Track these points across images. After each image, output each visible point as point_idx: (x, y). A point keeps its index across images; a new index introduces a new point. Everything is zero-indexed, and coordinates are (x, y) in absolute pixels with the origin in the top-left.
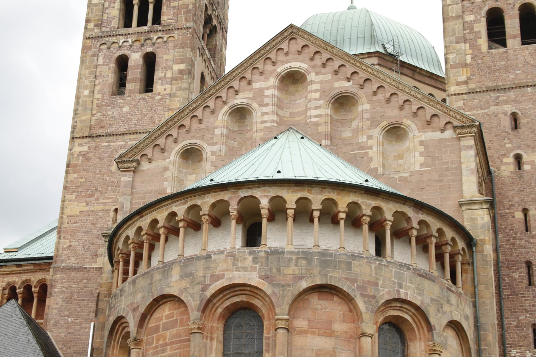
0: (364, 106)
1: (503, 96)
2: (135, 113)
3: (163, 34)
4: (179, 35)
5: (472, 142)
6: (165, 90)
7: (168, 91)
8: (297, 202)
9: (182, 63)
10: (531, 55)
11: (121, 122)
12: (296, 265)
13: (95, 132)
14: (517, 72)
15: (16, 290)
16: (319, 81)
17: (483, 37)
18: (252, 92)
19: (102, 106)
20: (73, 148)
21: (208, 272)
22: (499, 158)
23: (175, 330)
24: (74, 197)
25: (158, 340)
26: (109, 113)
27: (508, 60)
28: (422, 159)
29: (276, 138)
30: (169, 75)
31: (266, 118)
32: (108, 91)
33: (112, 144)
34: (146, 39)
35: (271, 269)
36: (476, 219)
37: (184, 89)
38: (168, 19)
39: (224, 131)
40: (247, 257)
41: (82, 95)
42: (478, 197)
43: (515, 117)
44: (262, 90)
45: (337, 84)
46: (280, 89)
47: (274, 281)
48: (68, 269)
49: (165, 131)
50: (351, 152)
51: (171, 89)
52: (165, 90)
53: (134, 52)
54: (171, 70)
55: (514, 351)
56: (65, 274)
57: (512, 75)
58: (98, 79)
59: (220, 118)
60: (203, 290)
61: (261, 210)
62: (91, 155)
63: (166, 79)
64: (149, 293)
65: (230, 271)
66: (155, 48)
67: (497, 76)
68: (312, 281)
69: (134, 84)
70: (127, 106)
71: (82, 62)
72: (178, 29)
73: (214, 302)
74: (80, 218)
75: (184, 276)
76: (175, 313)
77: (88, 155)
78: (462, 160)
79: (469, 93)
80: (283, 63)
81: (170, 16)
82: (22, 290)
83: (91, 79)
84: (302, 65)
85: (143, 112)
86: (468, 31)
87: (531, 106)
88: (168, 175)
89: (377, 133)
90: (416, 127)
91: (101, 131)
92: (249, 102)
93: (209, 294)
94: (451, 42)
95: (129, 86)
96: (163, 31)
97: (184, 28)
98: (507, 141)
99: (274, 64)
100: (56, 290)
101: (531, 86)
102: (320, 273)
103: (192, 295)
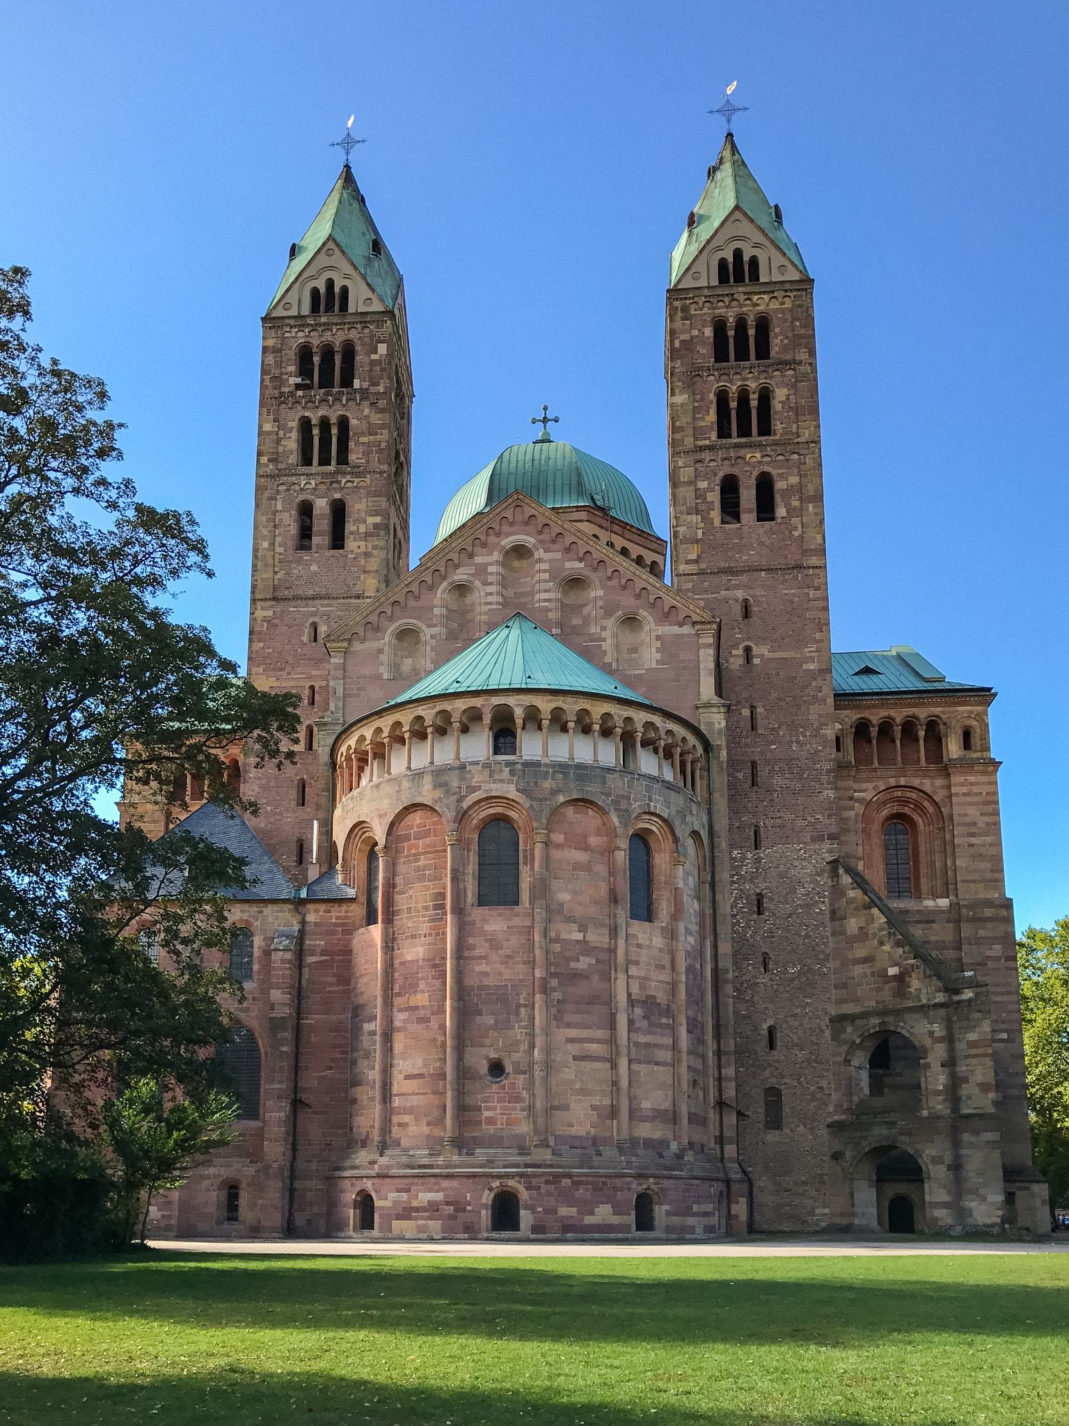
0: (596, 593)
4: (371, 479)
5: (711, 640)
6: (359, 547)
13: (279, 594)
23: (428, 840)
24: (261, 670)
25: (409, 850)
28: (658, 656)
30: (362, 529)
31: (490, 599)
32: (290, 543)
34: (333, 482)
39: (444, 611)
42: (716, 700)
44: (486, 565)
45: (568, 565)
46: (503, 565)
49: (377, 607)
52: (359, 547)
59: (439, 595)
60: (459, 801)
71: (257, 506)
75: (435, 787)
80: (508, 535)
84: (529, 541)
88: (383, 658)
89: (610, 623)
92: (471, 578)
93: (465, 805)
94: (682, 513)
99: (498, 535)
103: (447, 806)
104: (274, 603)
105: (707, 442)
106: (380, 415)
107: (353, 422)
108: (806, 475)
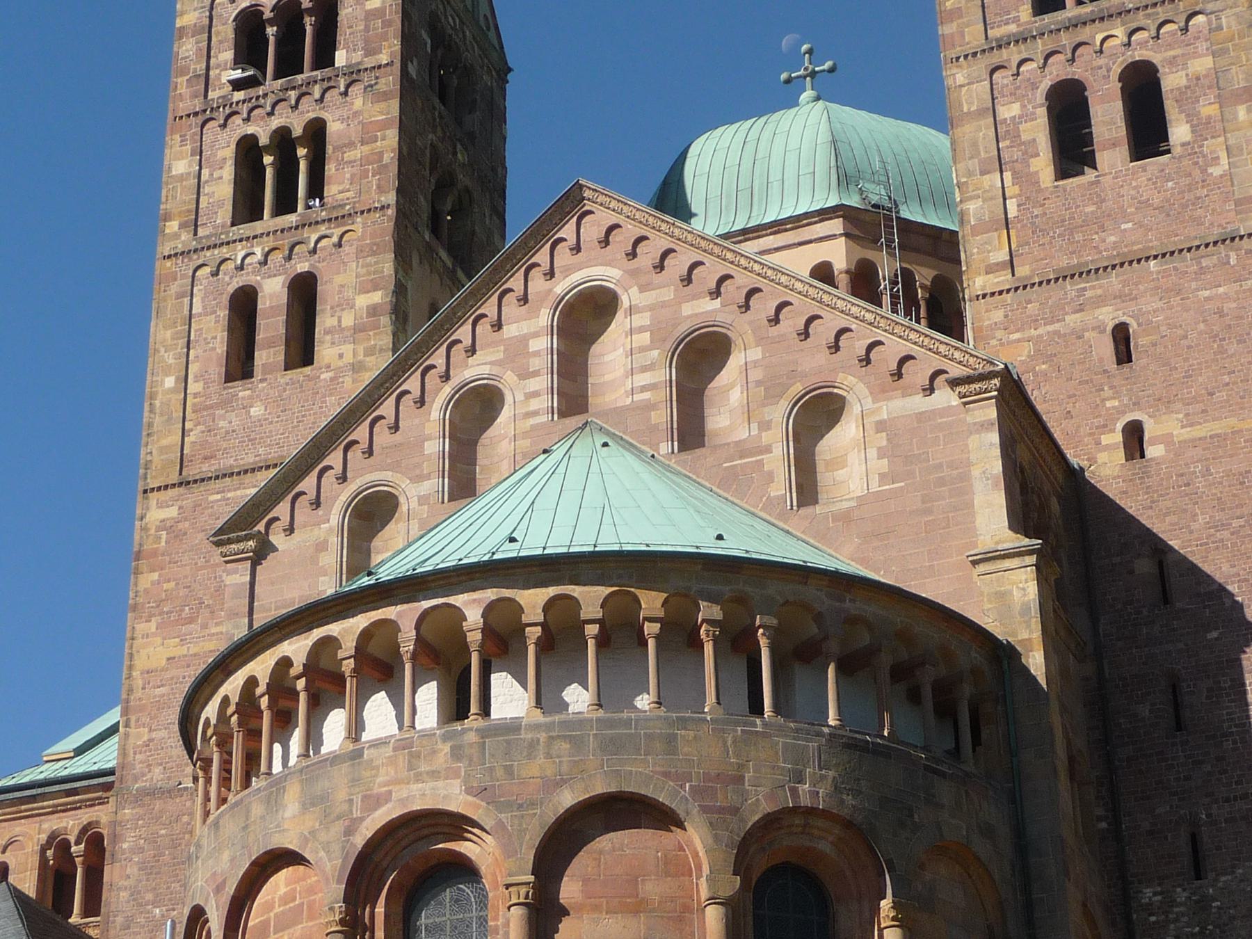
1: (1093, 288)
3: (330, 228)
4: (365, 225)
6: (341, 356)
7: (349, 358)
8: (549, 606)
10: (1155, 183)
11: (249, 440)
12: (548, 755)
13: (191, 472)
14: (1123, 227)
15: (70, 847)
16: (648, 306)
17: (1041, 154)
18: (502, 348)
19: (207, 408)
20: (145, 514)
21: (357, 790)
22: (1091, 434)
24: (153, 626)
26: (222, 424)
27: (1103, 201)
29: (545, 451)
30: (348, 320)
31: (535, 404)
33: (229, 495)
35: (491, 769)
36: (1011, 592)
37: (381, 350)
40: (440, 746)
41: (160, 390)
43: (1121, 335)
44: (524, 340)
45: (687, 309)
47: (500, 797)
48: (148, 794)
50: (725, 465)
52: (341, 356)
53: (269, 277)
54: (351, 308)
55: (1148, 892)
56: (142, 806)
57: (1112, 235)
60: (349, 832)
61: (468, 634)
62: (187, 524)
63: (343, 329)
64: (243, 847)
65: (403, 783)
66: (316, 262)
67: (1078, 242)
68: (586, 789)
69: (272, 350)
70: (259, 403)
72: (362, 212)
73: (376, 858)
74: (168, 675)
75: (308, 803)
76: (298, 889)
77: (180, 526)
78: (973, 457)
79: (1017, 289)
80: (568, 271)
81: (344, 182)
82: (82, 846)
83: (179, 350)
85: (294, 413)
86: (1008, 143)
87: (1160, 304)
89: (779, 413)
90: (867, 391)
91: (207, 468)
92: (496, 370)
93: (359, 841)
94: (970, 174)
95: (262, 357)
96: (330, 220)
97: (376, 208)
98: (1107, 392)
99: (551, 274)
100: (125, 846)
101: (1156, 257)
102: (603, 768)
103: (326, 847)
104: (182, 490)
105: (1013, 28)
106: (383, 105)
107: (334, 128)
108: (1225, 51)
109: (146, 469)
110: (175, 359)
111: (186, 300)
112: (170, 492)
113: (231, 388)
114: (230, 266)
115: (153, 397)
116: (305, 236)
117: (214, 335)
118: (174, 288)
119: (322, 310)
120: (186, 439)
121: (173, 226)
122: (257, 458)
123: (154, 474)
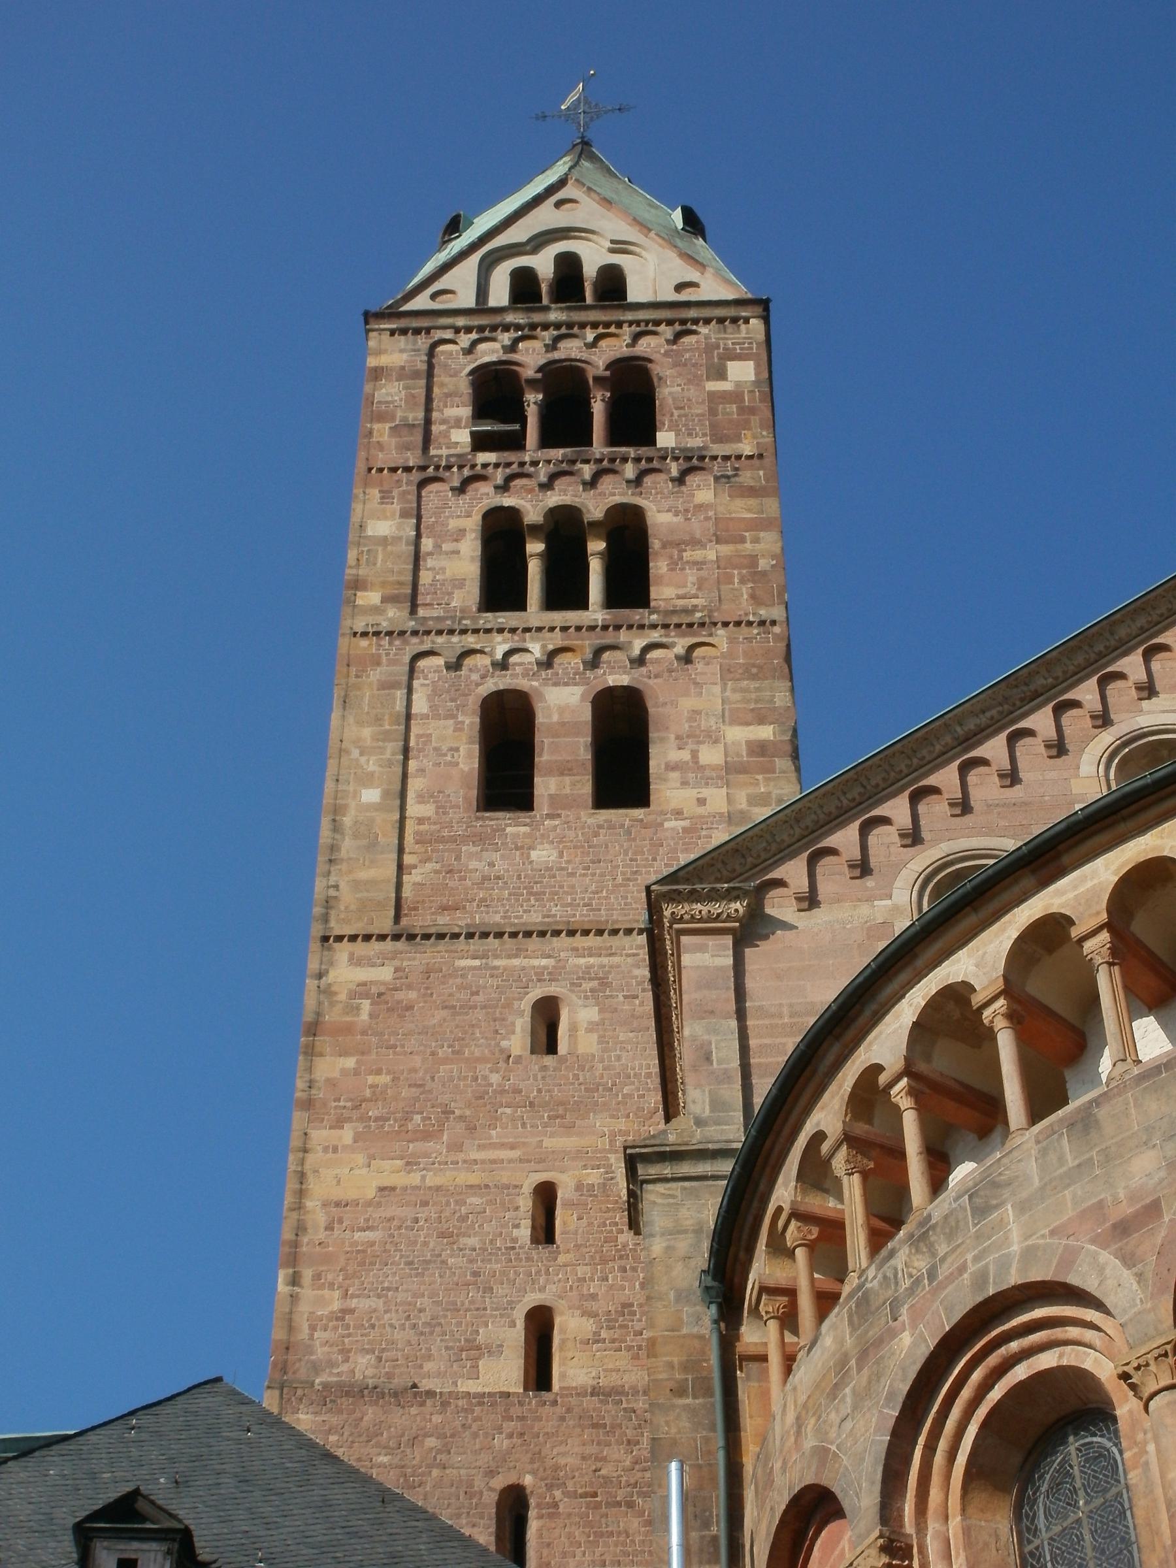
2: (588, 868)
3: (667, 636)
4: (732, 640)
9: (761, 720)
11: (531, 894)
19: (442, 840)
20: (327, 972)
33: (497, 963)
38: (679, 597)
41: (352, 804)
51: (730, 799)
53: (556, 684)
54: (716, 741)
58: (417, 758)
62: (413, 995)
63: (702, 768)
69: (567, 779)
74: (377, 1214)
77: (400, 995)
91: (443, 921)
95: (544, 786)
104: (401, 945)
109: (327, 908)
110: (380, 766)
111: (400, 694)
112: (375, 946)
113: (492, 820)
114: (482, 661)
115: (338, 810)
116: (622, 639)
117: (456, 745)
118: (375, 675)
119: (662, 740)
120: (405, 878)
121: (371, 597)
122: (547, 920)
123: (342, 916)
